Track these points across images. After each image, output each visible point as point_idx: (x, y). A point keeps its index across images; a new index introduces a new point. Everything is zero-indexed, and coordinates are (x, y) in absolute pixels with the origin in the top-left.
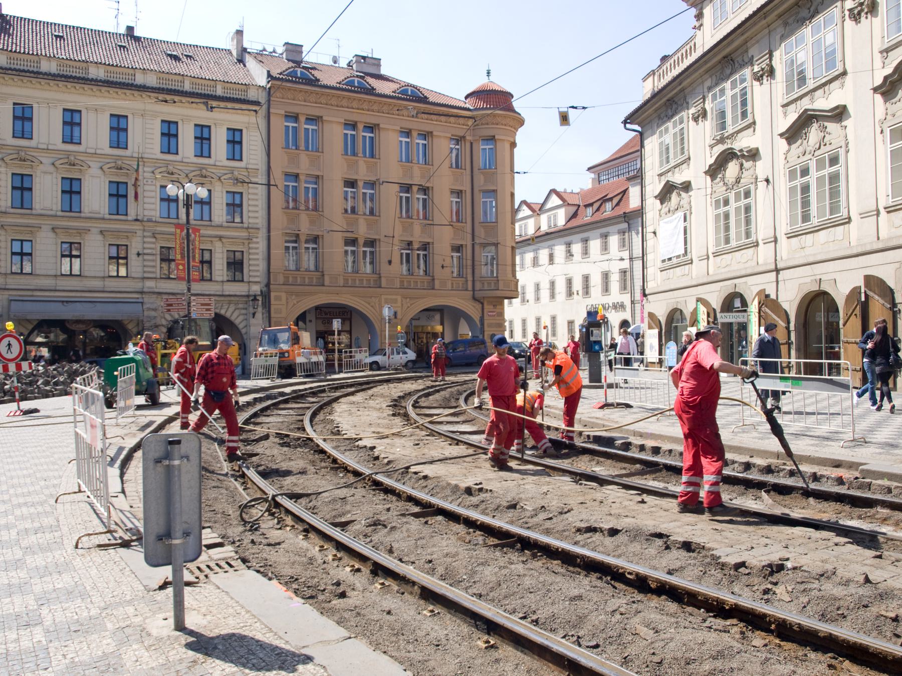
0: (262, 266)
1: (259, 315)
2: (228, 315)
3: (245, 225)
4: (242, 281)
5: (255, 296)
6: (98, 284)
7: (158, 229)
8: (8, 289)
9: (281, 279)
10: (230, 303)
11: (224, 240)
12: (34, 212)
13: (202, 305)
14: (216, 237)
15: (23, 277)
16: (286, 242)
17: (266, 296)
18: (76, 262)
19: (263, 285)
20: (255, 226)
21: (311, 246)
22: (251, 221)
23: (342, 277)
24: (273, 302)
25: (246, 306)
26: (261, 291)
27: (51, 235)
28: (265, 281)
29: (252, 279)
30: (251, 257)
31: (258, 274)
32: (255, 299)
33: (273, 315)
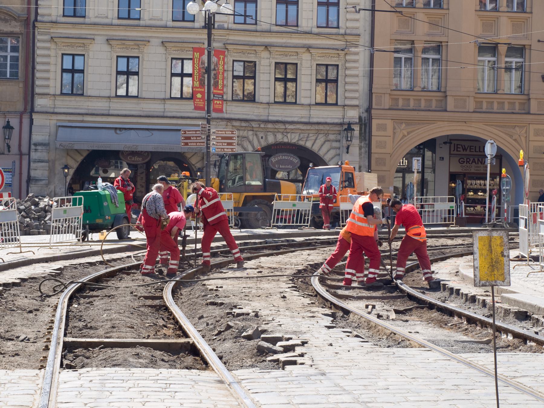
0: (362, 85)
1: (355, 150)
2: (315, 149)
3: (342, 31)
4: (336, 104)
5: (349, 124)
6: (156, 108)
7: (231, 38)
8: (56, 113)
9: (387, 102)
10: (318, 132)
11: (312, 51)
12: (87, 20)
13: (223, 138)
14: (303, 47)
15: (73, 98)
16: (397, 51)
17: (365, 124)
18: (133, 81)
19: (362, 110)
20: (355, 32)
21: (432, 56)
22: (349, 24)
23: (472, 99)
24: (374, 132)
25: (339, 137)
26: (360, 118)
27: (106, 48)
28: (366, 105)
29: (348, 102)
30: (348, 72)
31: (357, 95)
32: (349, 128)
33: (374, 149)
